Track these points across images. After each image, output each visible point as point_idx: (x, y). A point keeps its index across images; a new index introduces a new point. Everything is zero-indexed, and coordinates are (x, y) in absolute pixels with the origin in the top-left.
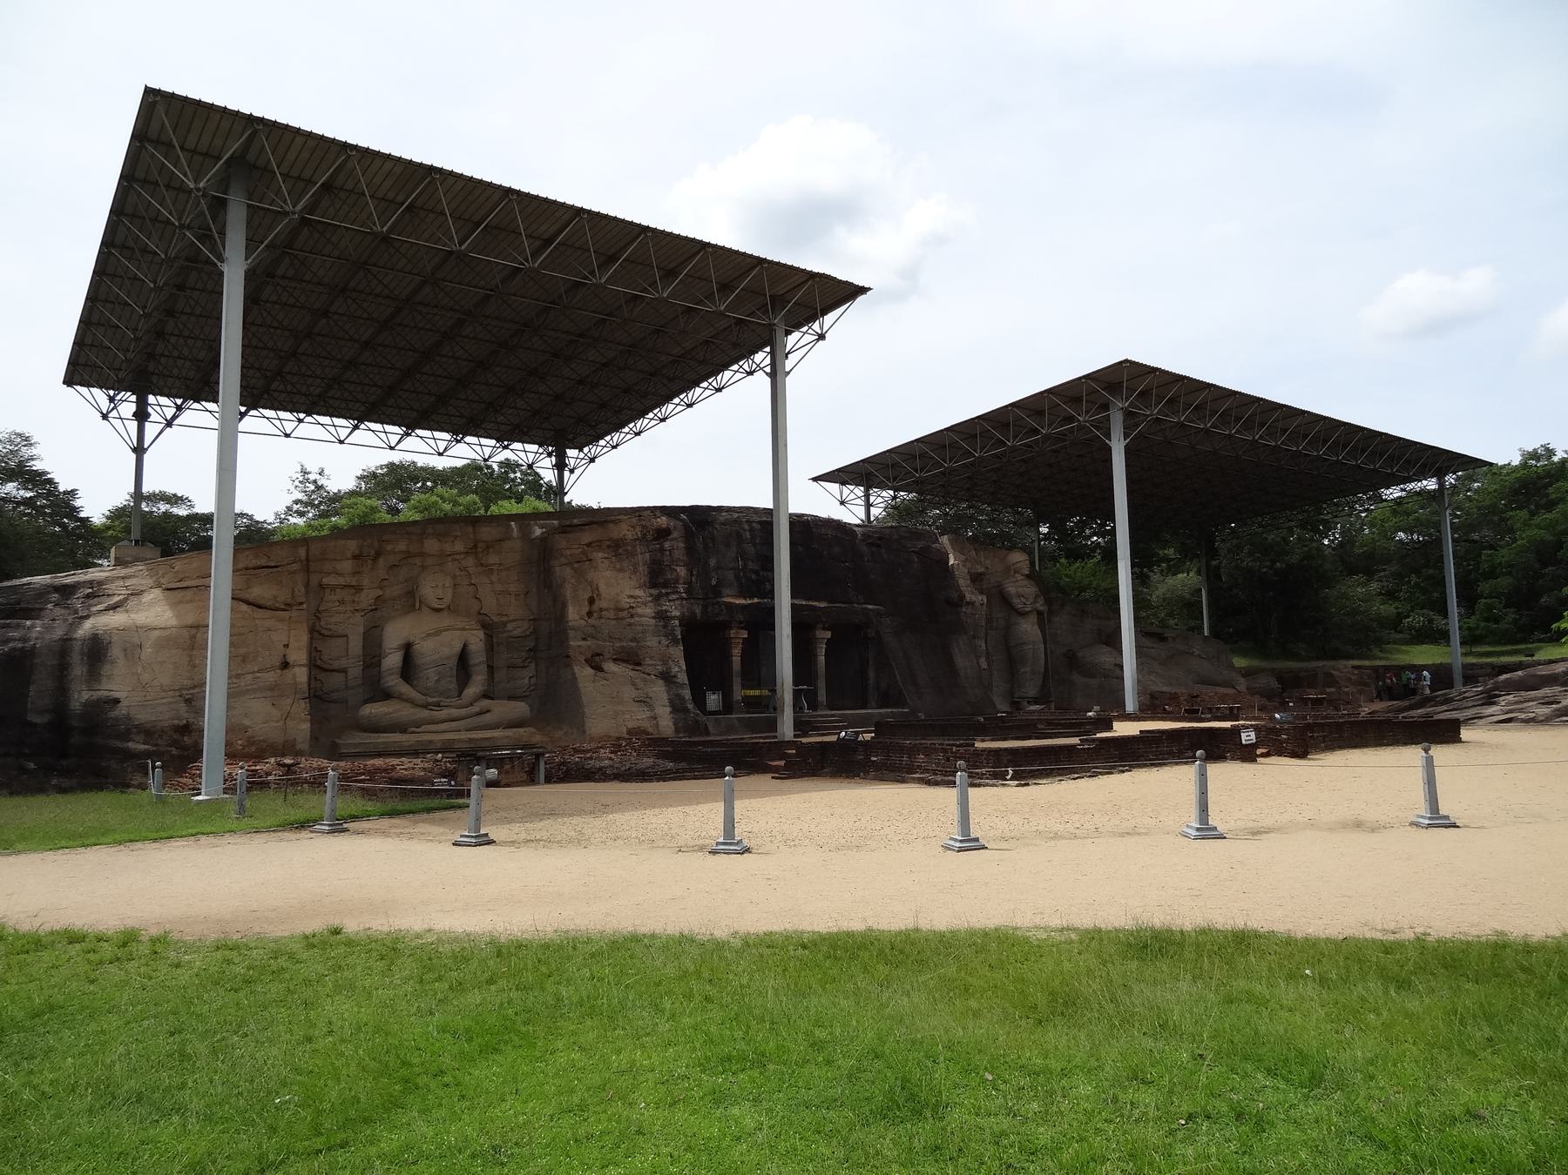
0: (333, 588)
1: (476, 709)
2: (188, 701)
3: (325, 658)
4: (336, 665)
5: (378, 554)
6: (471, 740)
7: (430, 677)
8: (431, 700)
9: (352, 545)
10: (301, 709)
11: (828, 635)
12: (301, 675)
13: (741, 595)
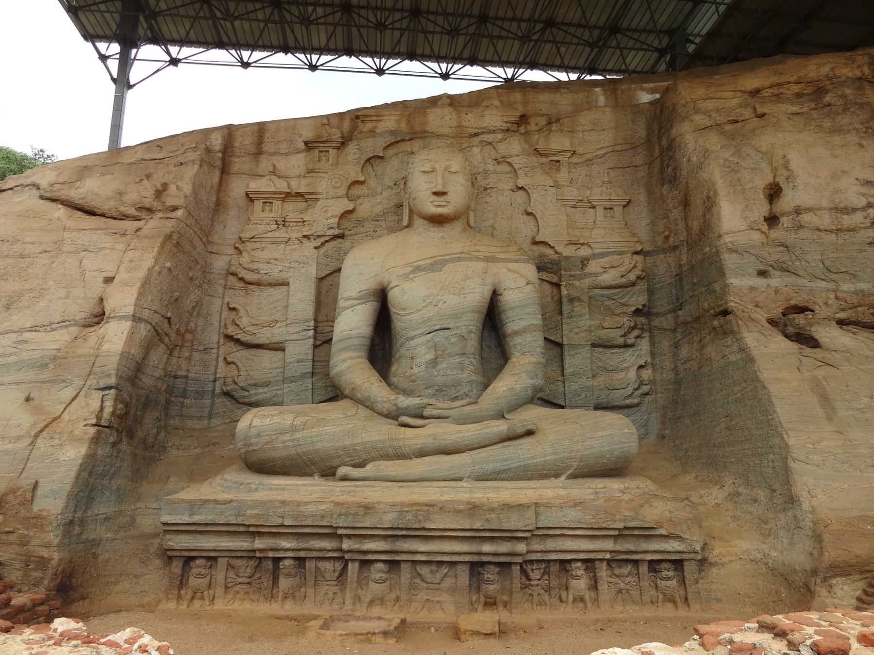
0: (268, 200)
1: (500, 427)
3: (244, 321)
4: (263, 336)
6: (474, 508)
7: (415, 352)
8: (405, 402)
10: (85, 409)
12: (115, 338)
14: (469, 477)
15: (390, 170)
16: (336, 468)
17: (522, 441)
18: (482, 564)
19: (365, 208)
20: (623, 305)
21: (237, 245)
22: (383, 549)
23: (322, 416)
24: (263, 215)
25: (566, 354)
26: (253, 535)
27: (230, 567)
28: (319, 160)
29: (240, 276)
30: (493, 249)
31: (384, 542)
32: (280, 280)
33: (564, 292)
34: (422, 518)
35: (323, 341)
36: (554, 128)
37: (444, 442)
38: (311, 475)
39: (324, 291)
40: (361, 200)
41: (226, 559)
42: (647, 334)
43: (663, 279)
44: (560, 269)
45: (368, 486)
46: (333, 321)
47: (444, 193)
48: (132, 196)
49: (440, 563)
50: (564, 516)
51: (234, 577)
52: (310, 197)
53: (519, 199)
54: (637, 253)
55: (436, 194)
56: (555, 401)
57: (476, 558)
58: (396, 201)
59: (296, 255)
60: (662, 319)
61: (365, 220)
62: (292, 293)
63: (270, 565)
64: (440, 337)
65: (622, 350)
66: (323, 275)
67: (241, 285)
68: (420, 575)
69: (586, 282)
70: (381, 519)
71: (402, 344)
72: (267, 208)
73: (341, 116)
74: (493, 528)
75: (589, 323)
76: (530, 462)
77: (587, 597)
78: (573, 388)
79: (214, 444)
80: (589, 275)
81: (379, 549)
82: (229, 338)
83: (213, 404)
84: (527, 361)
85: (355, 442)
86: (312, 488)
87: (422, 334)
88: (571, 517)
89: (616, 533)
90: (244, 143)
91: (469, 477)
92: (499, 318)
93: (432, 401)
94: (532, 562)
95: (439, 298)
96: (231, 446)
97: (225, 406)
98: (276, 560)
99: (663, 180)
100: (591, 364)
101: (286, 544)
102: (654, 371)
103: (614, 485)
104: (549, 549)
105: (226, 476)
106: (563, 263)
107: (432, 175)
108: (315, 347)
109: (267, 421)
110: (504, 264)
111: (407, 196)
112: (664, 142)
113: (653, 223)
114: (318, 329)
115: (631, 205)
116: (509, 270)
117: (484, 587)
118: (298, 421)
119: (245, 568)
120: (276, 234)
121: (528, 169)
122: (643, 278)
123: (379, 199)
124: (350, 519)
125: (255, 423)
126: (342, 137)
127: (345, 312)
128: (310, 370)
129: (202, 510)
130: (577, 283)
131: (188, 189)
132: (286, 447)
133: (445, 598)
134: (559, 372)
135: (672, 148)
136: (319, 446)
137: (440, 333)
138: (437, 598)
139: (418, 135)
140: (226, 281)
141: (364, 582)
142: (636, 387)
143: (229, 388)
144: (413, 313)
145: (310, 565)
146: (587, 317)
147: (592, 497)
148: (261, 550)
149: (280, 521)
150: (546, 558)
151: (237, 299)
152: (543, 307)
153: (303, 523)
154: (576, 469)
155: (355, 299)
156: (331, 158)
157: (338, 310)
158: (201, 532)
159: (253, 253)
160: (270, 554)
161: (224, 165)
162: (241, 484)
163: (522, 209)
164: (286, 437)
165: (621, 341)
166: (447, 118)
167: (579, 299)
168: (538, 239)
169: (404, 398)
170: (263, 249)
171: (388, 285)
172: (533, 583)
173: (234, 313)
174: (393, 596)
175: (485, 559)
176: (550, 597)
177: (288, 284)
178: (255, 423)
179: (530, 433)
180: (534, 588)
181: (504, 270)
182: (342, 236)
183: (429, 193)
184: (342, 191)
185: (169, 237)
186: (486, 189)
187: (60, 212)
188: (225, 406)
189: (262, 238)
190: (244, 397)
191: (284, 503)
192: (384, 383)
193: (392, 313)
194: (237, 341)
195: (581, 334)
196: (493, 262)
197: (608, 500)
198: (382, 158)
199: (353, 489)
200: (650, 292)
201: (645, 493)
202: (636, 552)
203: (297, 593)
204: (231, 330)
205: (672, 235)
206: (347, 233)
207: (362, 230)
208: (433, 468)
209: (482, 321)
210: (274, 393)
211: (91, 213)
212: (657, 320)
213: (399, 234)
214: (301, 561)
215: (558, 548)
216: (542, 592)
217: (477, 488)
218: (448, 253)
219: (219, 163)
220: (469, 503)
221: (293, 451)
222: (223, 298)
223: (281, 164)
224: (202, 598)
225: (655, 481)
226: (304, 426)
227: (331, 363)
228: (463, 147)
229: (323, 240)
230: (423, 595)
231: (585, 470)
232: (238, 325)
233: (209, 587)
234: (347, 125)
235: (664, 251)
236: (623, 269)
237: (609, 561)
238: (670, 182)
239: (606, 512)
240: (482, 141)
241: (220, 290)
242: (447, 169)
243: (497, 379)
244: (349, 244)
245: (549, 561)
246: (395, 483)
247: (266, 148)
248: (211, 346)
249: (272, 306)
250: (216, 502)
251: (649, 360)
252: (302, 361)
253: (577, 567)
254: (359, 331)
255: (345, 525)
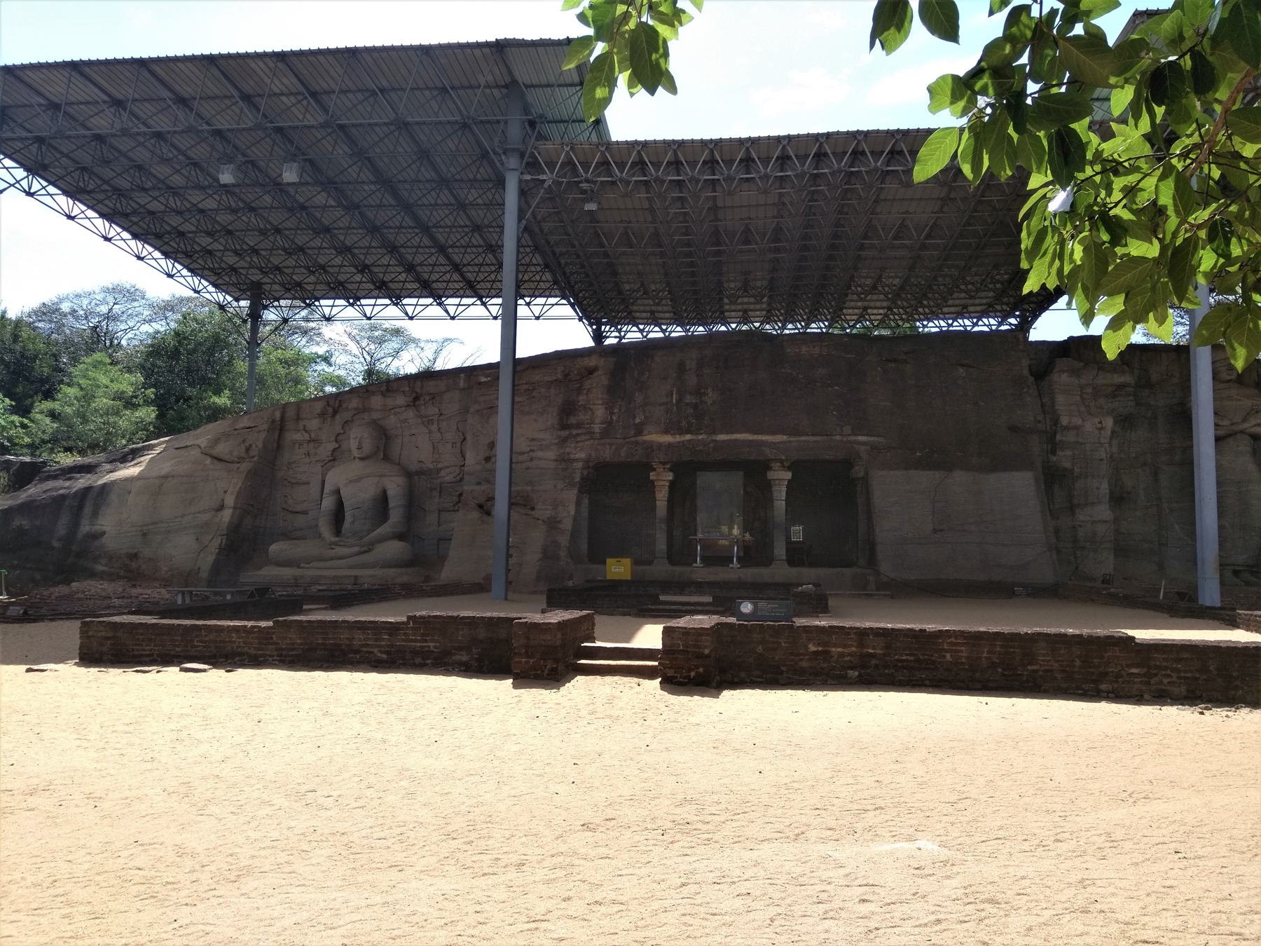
2: (144, 535)
3: (290, 501)
4: (298, 508)
5: (335, 412)
9: (319, 407)
10: (215, 544)
11: (789, 475)
12: (227, 515)
13: (666, 432)
48: (236, 453)
131: (260, 446)
178: (274, 548)
184: (333, 438)
185: (249, 472)
187: (208, 461)
211: (220, 460)
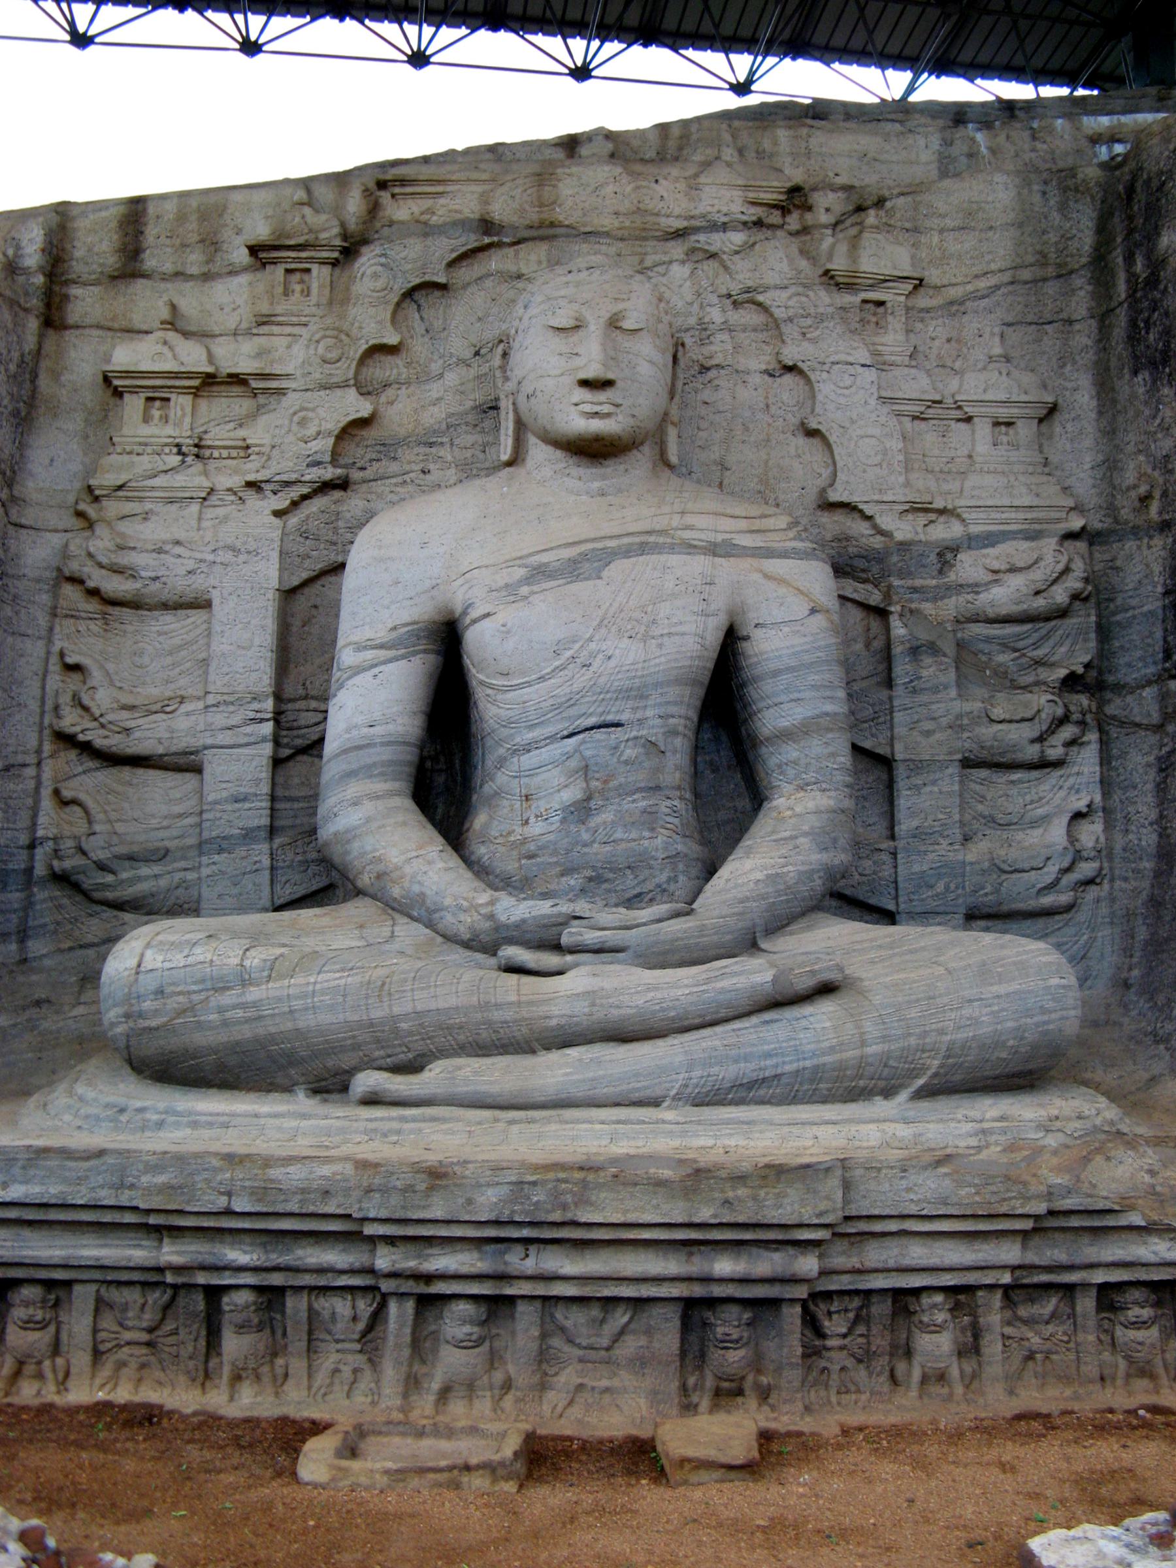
0: (157, 391)
1: (752, 974)
3: (102, 699)
4: (150, 735)
6: (698, 1177)
8: (514, 909)
14: (677, 1098)
15: (462, 320)
16: (351, 1072)
17: (807, 1010)
18: (712, 1303)
19: (403, 412)
20: (1038, 663)
21: (82, 506)
22: (473, 1270)
23: (310, 943)
24: (146, 430)
25: (901, 784)
26: (158, 1232)
27: (100, 1305)
28: (286, 293)
29: (91, 584)
30: (727, 524)
31: (476, 1255)
32: (190, 596)
33: (898, 629)
34: (569, 1198)
35: (296, 746)
36: (871, 217)
37: (615, 1013)
38: (288, 1089)
39: (296, 623)
40: (390, 392)
41: (93, 1288)
42: (1093, 736)
43: (1134, 602)
44: (885, 574)
45: (434, 1119)
46: (325, 698)
47: (607, 384)
49: (610, 1302)
50: (908, 1190)
51: (116, 1328)
52: (262, 384)
53: (785, 396)
54: (1071, 536)
55: (585, 383)
56: (873, 901)
57: (698, 1291)
58: (479, 396)
59: (228, 534)
60: (1129, 699)
61: (403, 442)
62: (217, 628)
63: (199, 1302)
64: (596, 745)
65: (1035, 774)
66: (296, 582)
67: (93, 606)
68: (563, 1329)
69: (951, 606)
70: (470, 1201)
71: (502, 762)
72: (156, 413)
73: (340, 179)
74: (741, 1219)
75: (958, 706)
76: (827, 1059)
77: (955, 1372)
78: (916, 868)
79: (38, 1003)
80: (960, 587)
81: (465, 1270)
82: (66, 739)
83: (28, 905)
84: (811, 805)
85: (397, 1010)
86: (294, 1123)
87: (552, 739)
88: (926, 1190)
89: (1028, 1225)
90: (95, 249)
91: (677, 1098)
92: (742, 698)
93: (581, 907)
94: (828, 1295)
95: (593, 646)
96: (80, 1010)
97: (60, 907)
98: (214, 1293)
99: (1136, 357)
100: (962, 810)
101: (238, 1255)
102: (1109, 826)
103: (1025, 1110)
104: (870, 1264)
105: (80, 1089)
106: (895, 559)
107: (575, 337)
108: (277, 762)
109: (178, 959)
110: (754, 562)
111: (510, 386)
112: (1139, 265)
113: (1110, 466)
114: (283, 718)
115: (1057, 417)
116: (766, 576)
117: (715, 1355)
118: (255, 959)
119: (140, 1308)
120: (179, 479)
121: (809, 321)
122: (1086, 599)
123: (435, 390)
124: (395, 1200)
125: (148, 964)
126: (345, 236)
127: (357, 680)
128: (265, 821)
129: (32, 1172)
130: (927, 608)
132: (225, 1023)
133: (625, 1379)
134: (881, 828)
135: (1158, 281)
136: (307, 1021)
137: (598, 735)
138: (605, 1383)
139: (534, 233)
140: (56, 596)
141: (428, 1344)
142: (1065, 864)
143: (68, 864)
144: (529, 684)
145: (296, 1305)
146: (953, 693)
147: (973, 1142)
148: (178, 1269)
149: (222, 1202)
150: (861, 1287)
151: (83, 642)
152: (847, 665)
153: (280, 1208)
154: (936, 1075)
155: (382, 647)
156: (315, 286)
157: (336, 674)
158: (30, 1223)
159: (124, 527)
160: (201, 1279)
161: (48, 305)
162: (122, 1111)
163: (795, 421)
164: (228, 999)
165: (1032, 752)
166: (610, 189)
167: (933, 649)
168: (834, 496)
169: (512, 901)
170: (146, 516)
171: (465, 613)
172: (830, 1343)
173: (76, 676)
174: (498, 1377)
175: (718, 1291)
176: (870, 1374)
177: (207, 605)
178: (146, 960)
179: (826, 989)
180: (832, 1354)
181: (756, 577)
182: (342, 485)
183: (569, 381)
186: (704, 369)
188: (60, 907)
189: (143, 489)
190: (106, 886)
191: (231, 1159)
192: (454, 860)
193: (474, 683)
194: (87, 748)
195: (938, 736)
196: (728, 555)
197: (1011, 1148)
198: (443, 287)
199: (395, 1125)
200: (1104, 632)
201: (1096, 1129)
202: (1071, 1268)
203: (265, 1369)
204: (71, 721)
205: (1157, 494)
206: (356, 475)
207: (394, 467)
208: (591, 1075)
209: (698, 703)
210: (178, 876)
212: (1118, 701)
213: (496, 484)
214: (271, 1297)
215: (891, 1263)
216: (849, 1363)
217: (699, 1123)
218: (616, 531)
219: (35, 302)
220: (681, 1162)
221: (246, 1033)
222: (50, 641)
223: (190, 300)
224: (40, 1376)
225: (1112, 1096)
226: (272, 970)
227: (322, 811)
228: (648, 263)
229: (295, 493)
230: (568, 1377)
231: (958, 1077)
232: (86, 709)
233: (56, 1349)
234: (354, 205)
235: (1136, 532)
236: (1039, 575)
237: (1007, 1289)
238: (1153, 365)
239: (1007, 1178)
240: (693, 250)
241: (43, 621)
242: (614, 323)
243: (739, 852)
244: (361, 504)
245: (868, 1293)
246: (497, 1113)
247: (150, 261)
248: (20, 759)
249: (169, 660)
250: (65, 1153)
251: (1098, 798)
252: (245, 799)
253: (935, 1306)
254: (391, 727)
255: (383, 1214)
